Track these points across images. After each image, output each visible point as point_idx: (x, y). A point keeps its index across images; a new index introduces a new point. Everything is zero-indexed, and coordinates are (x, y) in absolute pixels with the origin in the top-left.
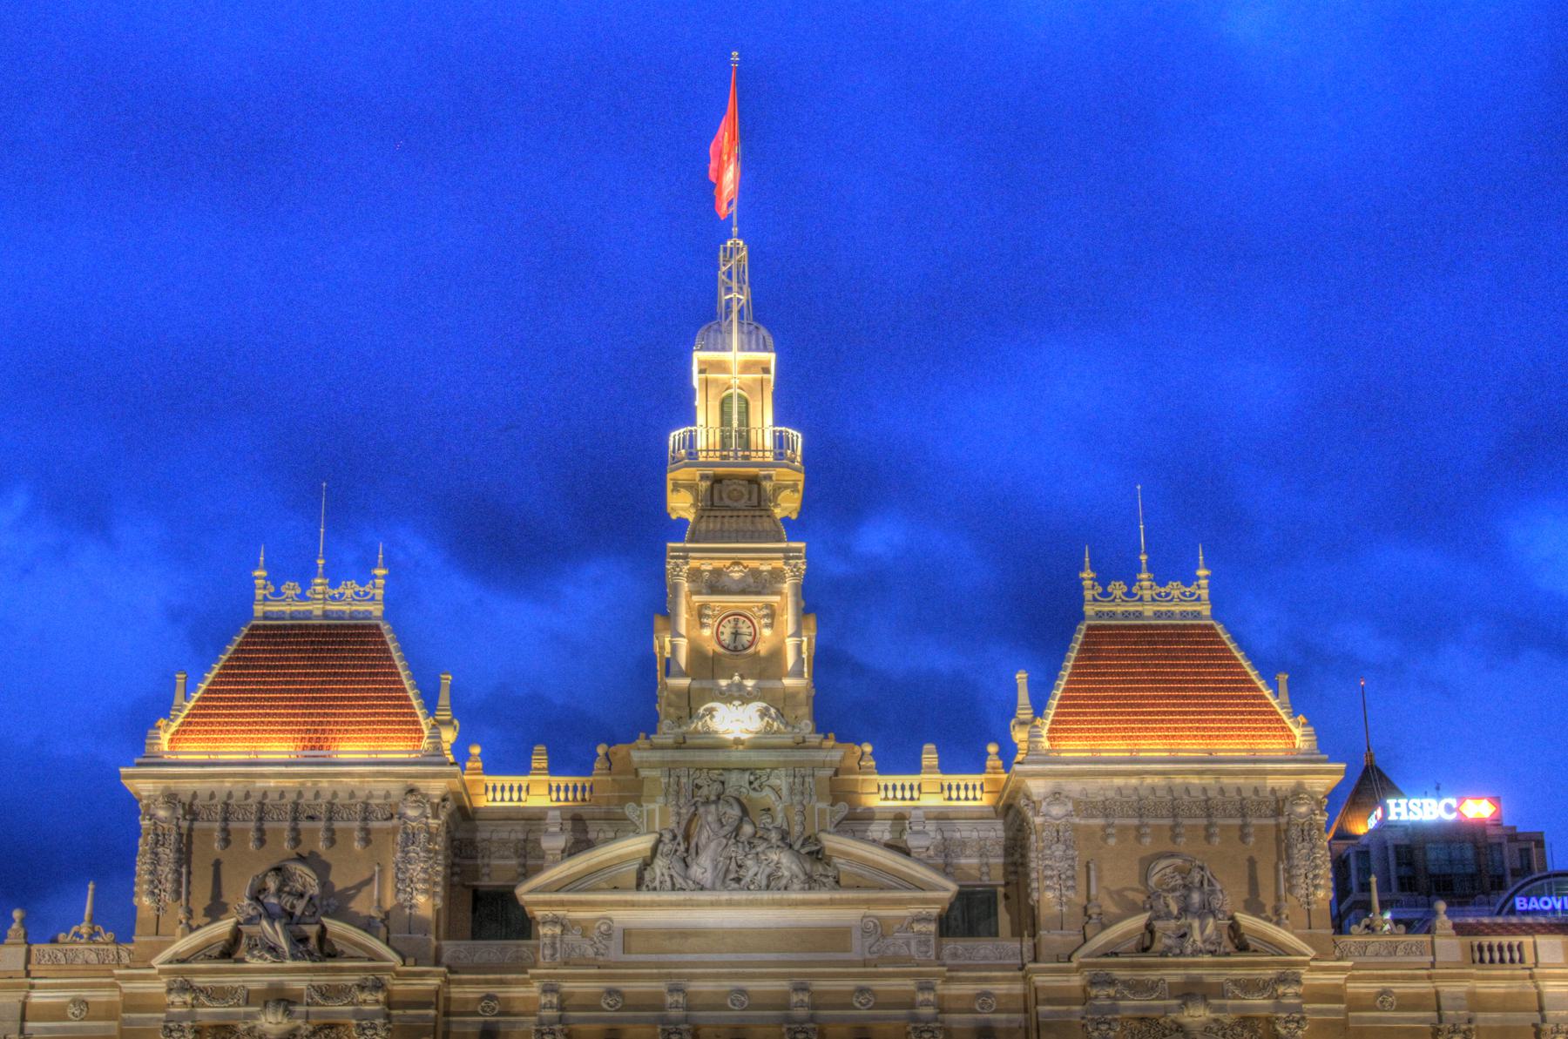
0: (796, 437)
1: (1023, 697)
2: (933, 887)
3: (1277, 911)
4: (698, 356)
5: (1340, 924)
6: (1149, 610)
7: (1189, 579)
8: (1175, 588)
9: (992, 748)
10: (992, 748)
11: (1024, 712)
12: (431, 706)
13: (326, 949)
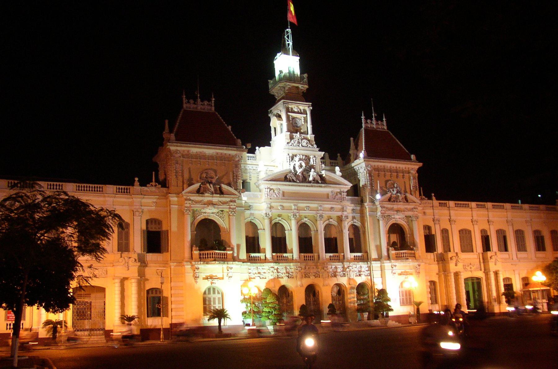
2: (346, 185)
13: (221, 192)
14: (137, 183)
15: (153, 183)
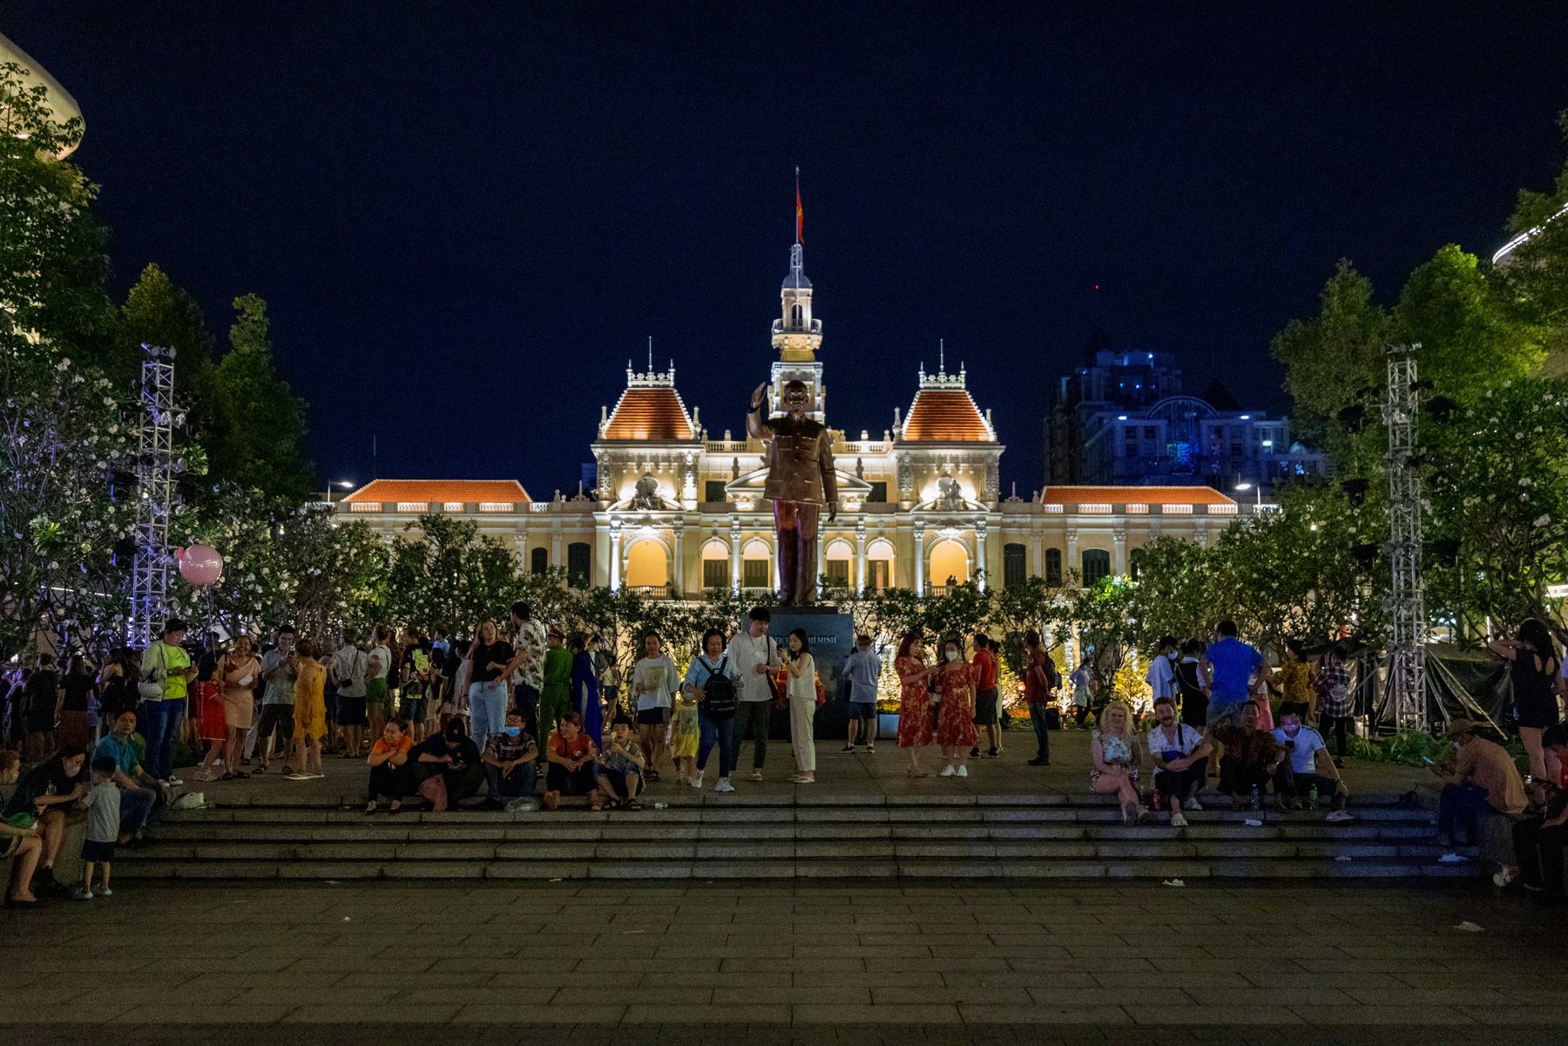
0: (819, 322)
1: (897, 416)
7: (958, 374)
8: (953, 378)
11: (897, 422)
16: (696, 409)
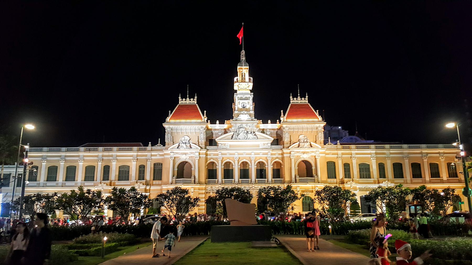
0: (252, 78)
3: (316, 142)
4: (238, 67)
5: (325, 144)
6: (299, 102)
9: (278, 121)
10: (278, 121)
12: (203, 115)
14: (150, 145)
15: (159, 144)
16: (205, 112)
